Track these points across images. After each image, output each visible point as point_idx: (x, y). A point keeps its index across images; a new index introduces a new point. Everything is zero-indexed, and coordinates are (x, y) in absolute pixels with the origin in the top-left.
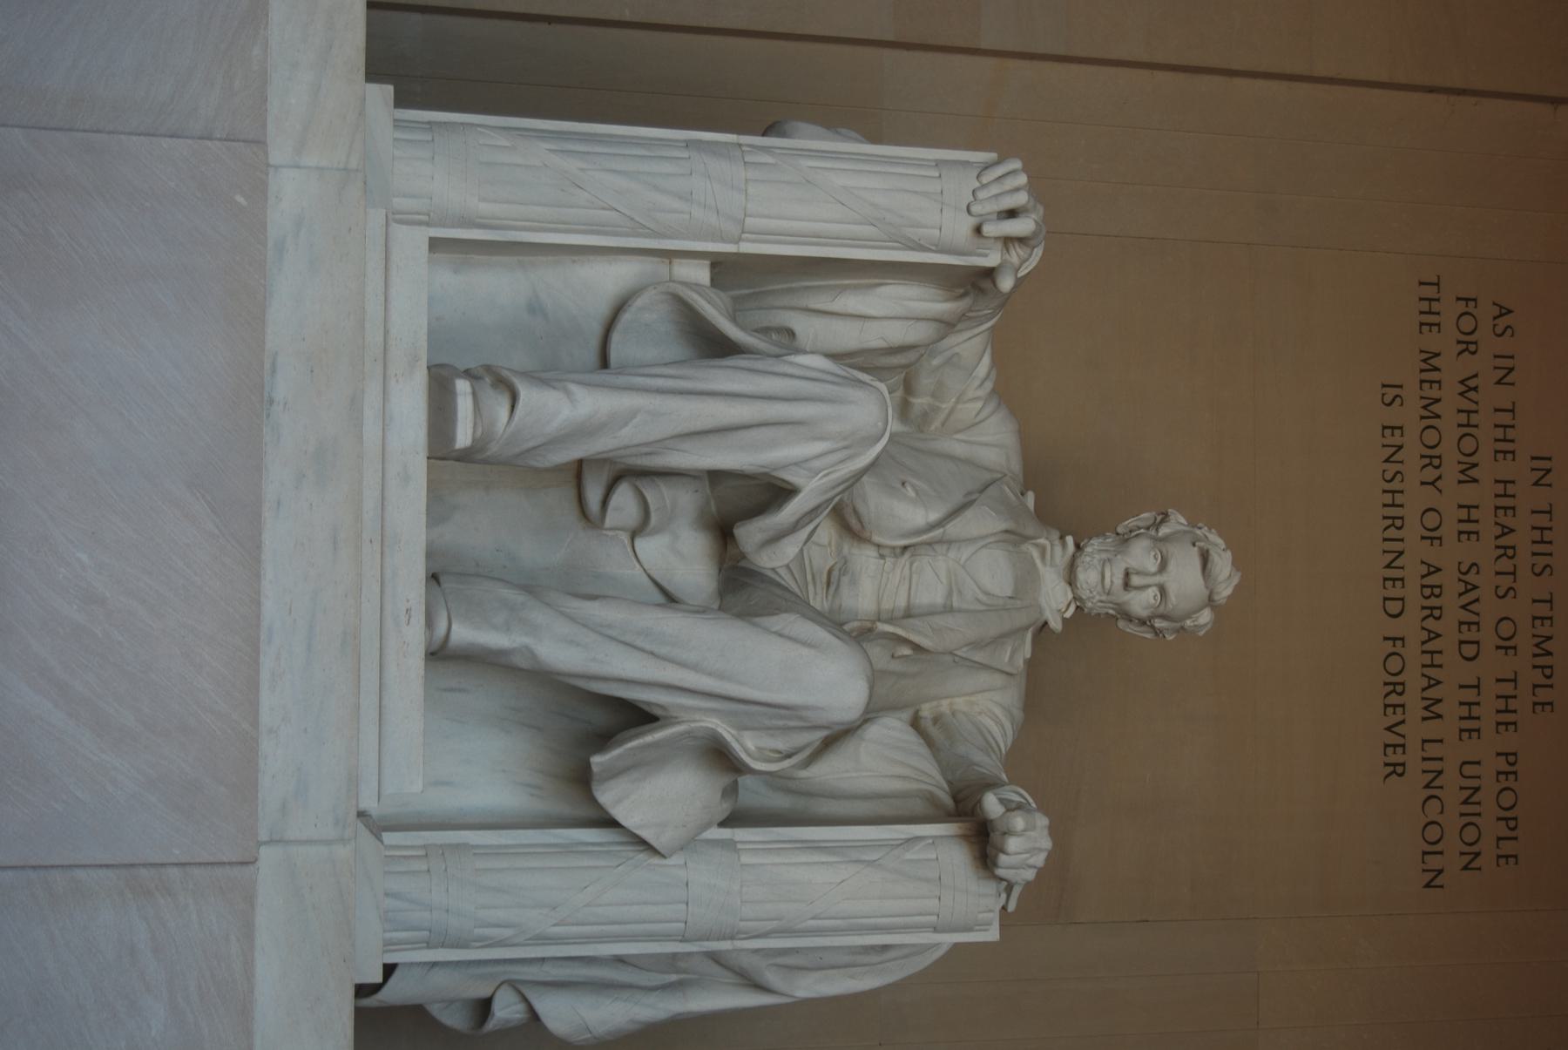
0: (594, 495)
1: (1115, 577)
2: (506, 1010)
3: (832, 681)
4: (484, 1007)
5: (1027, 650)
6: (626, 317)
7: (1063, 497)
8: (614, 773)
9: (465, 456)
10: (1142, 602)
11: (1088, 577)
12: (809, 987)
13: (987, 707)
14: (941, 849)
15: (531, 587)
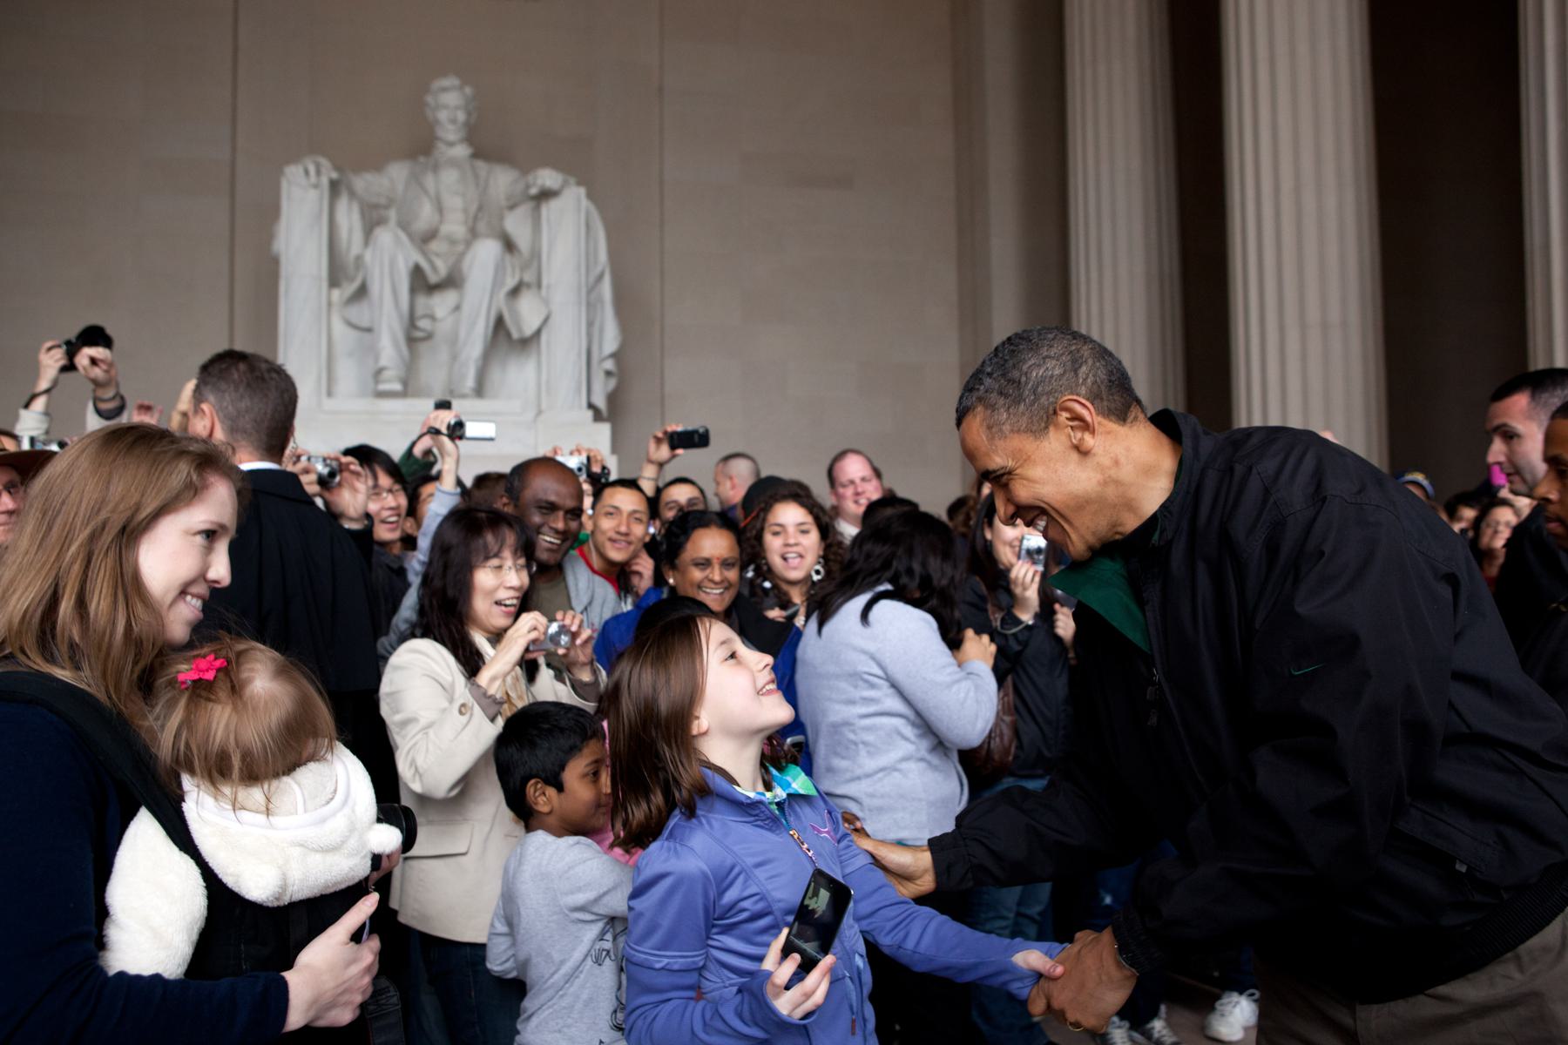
0: (419, 334)
1: (451, 127)
2: (609, 365)
3: (487, 251)
4: (608, 373)
5: (481, 165)
6: (355, 321)
7: (420, 146)
8: (520, 330)
9: (405, 383)
10: (461, 116)
11: (451, 137)
12: (603, 256)
13: (502, 180)
14: (550, 209)
15: (454, 357)
